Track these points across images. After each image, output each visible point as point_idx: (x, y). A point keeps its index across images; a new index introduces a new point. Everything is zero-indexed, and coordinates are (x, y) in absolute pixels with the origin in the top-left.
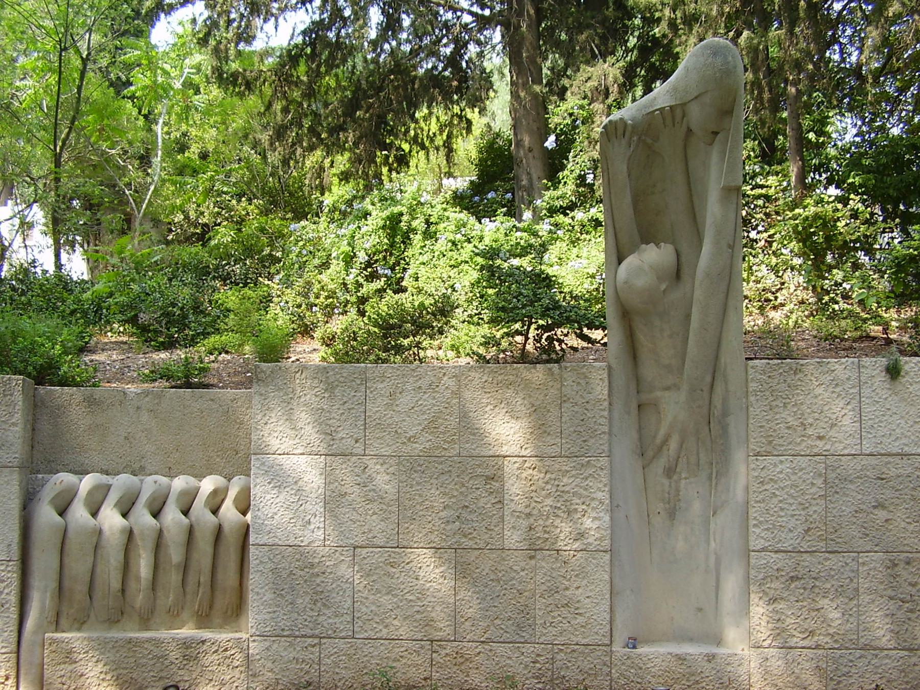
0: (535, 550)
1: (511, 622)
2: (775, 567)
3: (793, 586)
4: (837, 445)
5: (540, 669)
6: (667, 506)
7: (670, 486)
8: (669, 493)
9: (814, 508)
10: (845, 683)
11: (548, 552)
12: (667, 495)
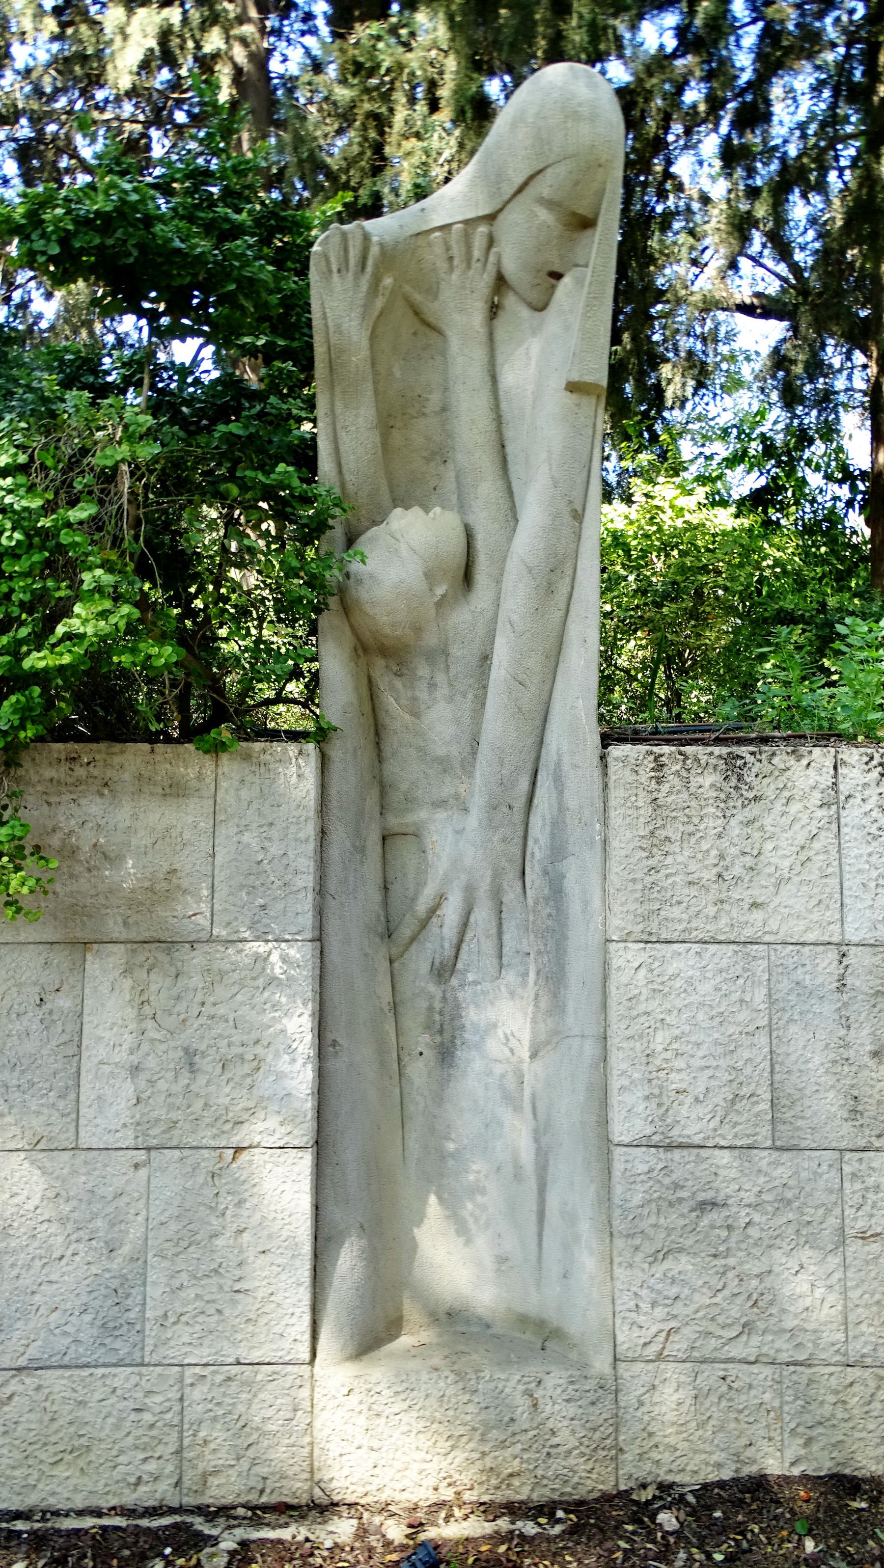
0: (148, 1149)
1: (87, 1318)
2: (667, 1181)
3: (705, 1222)
4: (792, 922)
5: (152, 1426)
6: (438, 1039)
7: (444, 998)
8: (441, 1013)
9: (746, 1055)
10: (823, 1441)
11: (177, 1153)
12: (437, 1017)
